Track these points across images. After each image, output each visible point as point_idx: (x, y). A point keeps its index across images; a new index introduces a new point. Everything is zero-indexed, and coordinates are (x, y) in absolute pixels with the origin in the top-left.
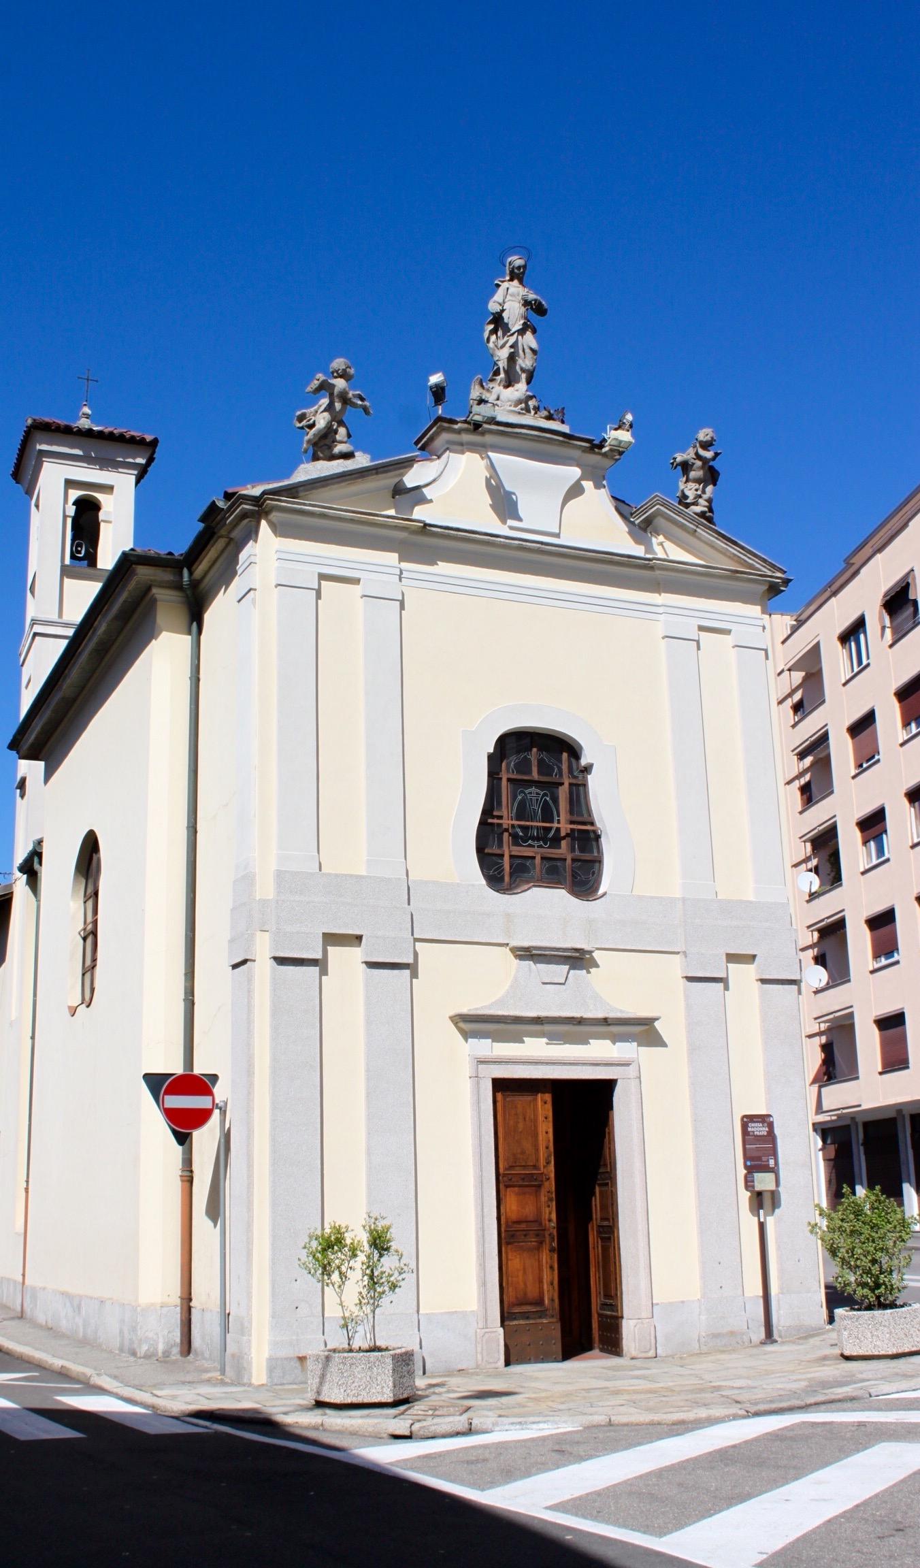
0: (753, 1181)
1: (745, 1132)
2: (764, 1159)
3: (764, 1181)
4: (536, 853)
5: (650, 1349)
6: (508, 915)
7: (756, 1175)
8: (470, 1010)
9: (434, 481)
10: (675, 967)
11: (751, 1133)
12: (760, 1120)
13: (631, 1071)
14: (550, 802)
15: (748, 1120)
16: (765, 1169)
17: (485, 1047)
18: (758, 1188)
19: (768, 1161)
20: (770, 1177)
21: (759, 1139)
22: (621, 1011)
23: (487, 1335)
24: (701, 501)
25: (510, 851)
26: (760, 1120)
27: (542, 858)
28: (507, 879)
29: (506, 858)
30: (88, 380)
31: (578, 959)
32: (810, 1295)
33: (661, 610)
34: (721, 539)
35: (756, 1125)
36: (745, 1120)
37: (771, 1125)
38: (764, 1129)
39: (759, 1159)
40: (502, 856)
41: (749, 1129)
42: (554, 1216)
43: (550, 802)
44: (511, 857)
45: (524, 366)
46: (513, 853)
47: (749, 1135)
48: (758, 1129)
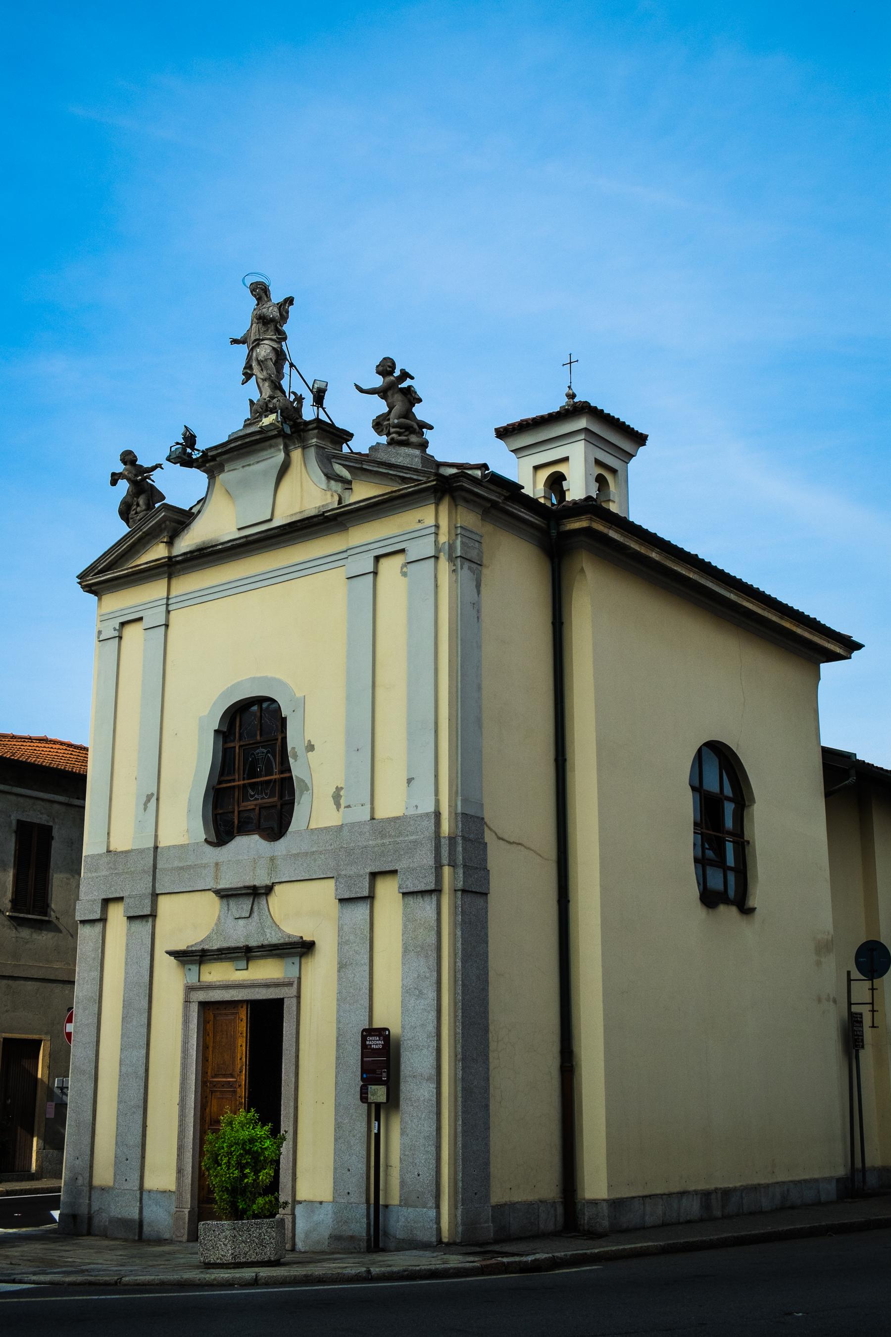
1: (364, 1046)
2: (378, 1071)
3: (379, 1093)
4: (256, 805)
7: (369, 1086)
11: (369, 1047)
12: (377, 1033)
14: (272, 758)
15: (369, 1032)
16: (378, 1082)
18: (371, 1098)
19: (381, 1074)
21: (376, 1052)
23: (178, 1213)
26: (377, 1033)
35: (374, 1038)
36: (365, 1033)
38: (380, 1042)
39: (374, 1072)
41: (367, 1043)
43: (272, 758)
44: (239, 812)
45: (262, 377)
47: (367, 1049)
48: (376, 1043)
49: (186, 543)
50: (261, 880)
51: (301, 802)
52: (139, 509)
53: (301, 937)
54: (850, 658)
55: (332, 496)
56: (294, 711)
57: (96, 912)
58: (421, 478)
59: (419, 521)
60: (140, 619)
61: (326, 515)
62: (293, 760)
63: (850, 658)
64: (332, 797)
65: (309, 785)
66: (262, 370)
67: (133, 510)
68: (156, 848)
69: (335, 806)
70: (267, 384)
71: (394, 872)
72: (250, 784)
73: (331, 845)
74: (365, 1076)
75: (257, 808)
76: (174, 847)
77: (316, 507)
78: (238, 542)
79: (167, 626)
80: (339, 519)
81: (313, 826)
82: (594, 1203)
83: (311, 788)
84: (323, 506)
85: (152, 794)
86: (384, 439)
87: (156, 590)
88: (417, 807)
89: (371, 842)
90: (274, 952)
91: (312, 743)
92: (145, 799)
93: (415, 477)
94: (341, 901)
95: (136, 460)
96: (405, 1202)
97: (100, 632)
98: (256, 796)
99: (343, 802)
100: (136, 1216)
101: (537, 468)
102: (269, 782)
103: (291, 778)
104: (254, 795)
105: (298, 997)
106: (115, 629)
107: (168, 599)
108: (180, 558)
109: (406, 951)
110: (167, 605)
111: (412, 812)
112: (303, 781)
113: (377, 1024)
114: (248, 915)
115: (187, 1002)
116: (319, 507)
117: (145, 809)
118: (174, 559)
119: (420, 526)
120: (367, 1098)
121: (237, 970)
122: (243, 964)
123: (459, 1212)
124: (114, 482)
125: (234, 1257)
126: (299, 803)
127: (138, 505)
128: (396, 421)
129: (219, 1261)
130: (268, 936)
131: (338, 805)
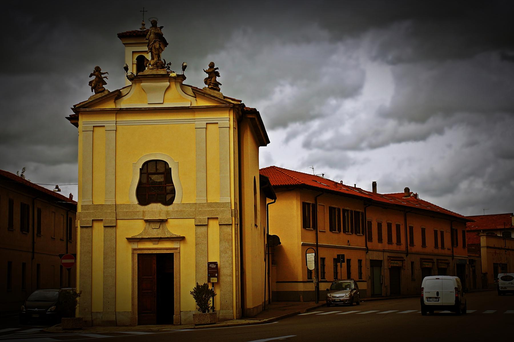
0: (210, 280)
5: (179, 323)
8: (132, 237)
13: (178, 251)
17: (135, 246)
20: (216, 279)
24: (211, 84)
29: (147, 195)
30: (144, 11)
31: (163, 222)
32: (229, 310)
33: (196, 120)
37: (217, 265)
40: (146, 195)
42: (156, 288)
44: (148, 195)
45: (155, 53)
49: (123, 104)
52: (99, 87)
53: (180, 235)
54: (266, 146)
57: (90, 225)
60: (104, 126)
63: (266, 146)
66: (156, 51)
68: (116, 204)
70: (157, 56)
71: (217, 218)
72: (152, 187)
74: (209, 275)
75: (156, 195)
79: (116, 130)
81: (182, 203)
82: (249, 309)
86: (207, 86)
87: (112, 119)
93: (225, 103)
94: (196, 225)
95: (101, 70)
96: (221, 309)
98: (155, 190)
100: (115, 319)
101: (133, 52)
102: (161, 186)
104: (154, 190)
105: (179, 253)
107: (116, 121)
108: (125, 109)
110: (116, 123)
113: (210, 261)
114: (158, 228)
115: (133, 254)
120: (210, 281)
123: (238, 310)
124: (90, 76)
125: (211, 322)
127: (99, 85)
128: (214, 82)
129: (205, 323)
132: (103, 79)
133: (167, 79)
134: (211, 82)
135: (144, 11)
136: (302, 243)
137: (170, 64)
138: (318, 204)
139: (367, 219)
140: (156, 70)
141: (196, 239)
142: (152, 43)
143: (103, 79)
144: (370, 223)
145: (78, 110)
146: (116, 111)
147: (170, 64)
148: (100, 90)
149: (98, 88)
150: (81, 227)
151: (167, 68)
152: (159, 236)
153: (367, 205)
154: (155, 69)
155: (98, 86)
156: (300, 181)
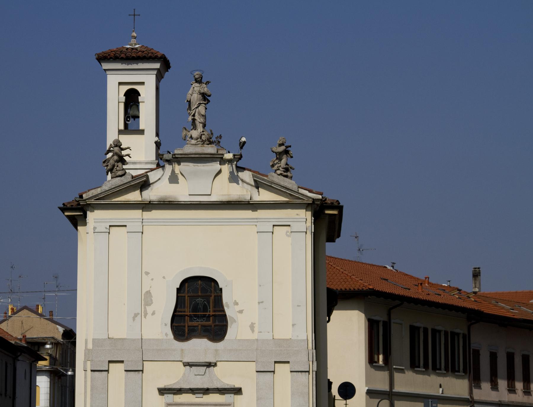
4: (199, 324)
6: (182, 350)
9: (159, 179)
10: (252, 367)
14: (207, 304)
22: (228, 385)
24: (280, 168)
25: (188, 324)
27: (201, 326)
28: (186, 335)
29: (186, 327)
30: (134, 15)
33: (258, 220)
34: (283, 188)
40: (185, 326)
43: (207, 304)
44: (188, 326)
45: (200, 121)
46: (189, 325)
50: (212, 360)
51: (232, 327)
52: (118, 168)
55: (247, 191)
56: (226, 286)
58: (304, 198)
59: (297, 214)
60: (126, 226)
61: (250, 202)
62: (227, 308)
64: (250, 326)
65: (236, 320)
67: (115, 169)
69: (251, 331)
70: (201, 125)
71: (288, 362)
73: (250, 347)
75: (200, 327)
76: (153, 339)
77: (237, 195)
78: (194, 203)
80: (254, 205)
81: (238, 338)
83: (237, 321)
84: (242, 195)
85: (138, 314)
88: (298, 336)
89: (273, 349)
90: (222, 391)
91: (237, 302)
92: (133, 315)
97: (95, 228)
98: (197, 320)
99: (256, 330)
101: (120, 84)
103: (226, 315)
104: (196, 319)
106: (106, 228)
108: (156, 203)
109: (293, 394)
110: (142, 222)
111: (295, 338)
112: (233, 318)
116: (240, 195)
117: (134, 320)
118: (151, 202)
119: (297, 217)
121: (196, 398)
122: (201, 395)
126: (230, 327)
127: (117, 166)
130: (215, 384)
131: (253, 331)
132: (124, 157)
133: (216, 161)
134: (280, 166)
135: (134, 15)
136: (367, 388)
137: (220, 137)
138: (392, 321)
139: (472, 345)
140: (202, 146)
141: (257, 392)
142: (196, 106)
143: (124, 157)
144: (477, 353)
145: (88, 202)
146: (144, 205)
147: (220, 137)
148: (120, 173)
149: (117, 170)
150: (92, 371)
151: (215, 143)
152: (205, 386)
153: (473, 321)
154: (199, 145)
155: (116, 167)
156: (365, 284)
